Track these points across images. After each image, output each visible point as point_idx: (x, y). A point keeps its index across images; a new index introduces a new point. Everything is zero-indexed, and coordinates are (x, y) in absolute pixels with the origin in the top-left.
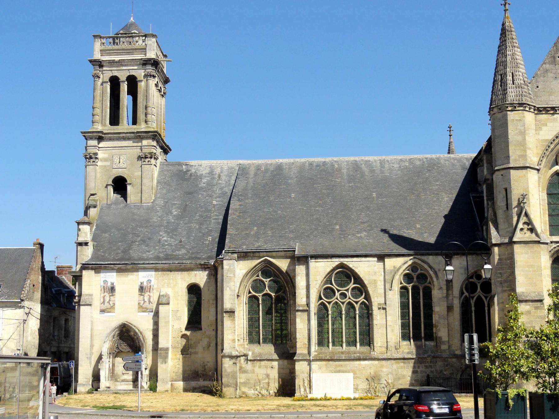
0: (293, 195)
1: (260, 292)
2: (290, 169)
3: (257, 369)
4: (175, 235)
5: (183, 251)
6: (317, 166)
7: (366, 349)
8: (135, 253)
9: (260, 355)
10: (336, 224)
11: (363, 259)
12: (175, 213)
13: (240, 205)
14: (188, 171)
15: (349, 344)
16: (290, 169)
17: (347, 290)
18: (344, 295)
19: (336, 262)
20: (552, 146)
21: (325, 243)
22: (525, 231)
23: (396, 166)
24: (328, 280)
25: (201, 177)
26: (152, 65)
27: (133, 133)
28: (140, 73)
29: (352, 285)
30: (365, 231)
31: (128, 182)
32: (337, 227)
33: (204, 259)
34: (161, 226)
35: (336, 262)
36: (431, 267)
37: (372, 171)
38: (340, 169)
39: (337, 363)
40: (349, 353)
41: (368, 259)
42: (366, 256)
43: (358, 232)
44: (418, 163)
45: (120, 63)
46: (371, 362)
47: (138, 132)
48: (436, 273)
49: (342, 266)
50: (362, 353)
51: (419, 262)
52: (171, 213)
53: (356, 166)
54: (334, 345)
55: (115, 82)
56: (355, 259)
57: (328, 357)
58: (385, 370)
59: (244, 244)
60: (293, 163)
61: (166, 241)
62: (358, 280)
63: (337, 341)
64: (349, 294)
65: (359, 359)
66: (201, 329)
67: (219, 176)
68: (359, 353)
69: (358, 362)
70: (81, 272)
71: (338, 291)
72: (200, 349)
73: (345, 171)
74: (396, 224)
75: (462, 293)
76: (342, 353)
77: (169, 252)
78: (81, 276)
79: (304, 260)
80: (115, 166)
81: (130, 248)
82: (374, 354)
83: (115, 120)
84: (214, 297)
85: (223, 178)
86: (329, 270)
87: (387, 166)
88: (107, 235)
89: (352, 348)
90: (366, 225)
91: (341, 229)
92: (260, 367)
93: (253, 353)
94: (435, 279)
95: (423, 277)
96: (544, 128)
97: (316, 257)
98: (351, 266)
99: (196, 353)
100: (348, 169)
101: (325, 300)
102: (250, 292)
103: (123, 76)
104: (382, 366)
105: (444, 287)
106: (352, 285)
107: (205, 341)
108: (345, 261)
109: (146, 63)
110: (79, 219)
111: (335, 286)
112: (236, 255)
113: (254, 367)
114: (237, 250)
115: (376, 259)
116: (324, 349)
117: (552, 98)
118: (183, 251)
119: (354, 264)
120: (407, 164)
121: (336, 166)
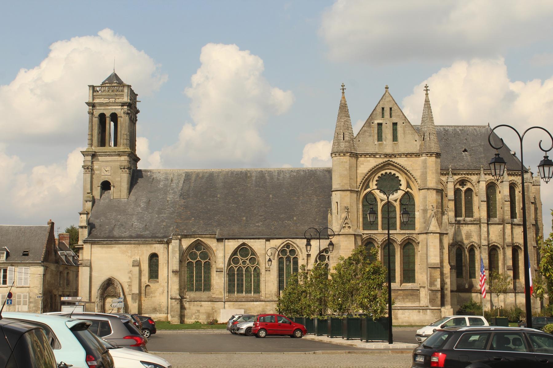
0: (219, 196)
1: (194, 260)
2: (218, 176)
3: (192, 307)
4: (143, 221)
5: (147, 232)
6: (236, 174)
7: (256, 295)
8: (116, 233)
9: (194, 298)
10: (244, 216)
11: (257, 240)
12: (142, 206)
13: (184, 202)
14: (151, 176)
15: (247, 292)
16: (218, 176)
17: (247, 259)
18: (244, 262)
19: (241, 242)
20: (366, 177)
21: (236, 229)
22: (347, 228)
23: (288, 175)
24: (235, 253)
25: (159, 181)
26: (128, 106)
27: (115, 152)
28: (120, 111)
29: (249, 257)
30: (261, 221)
31: (112, 184)
32: (244, 218)
33: (160, 238)
34: (133, 215)
35: (241, 242)
36: (298, 246)
37: (272, 178)
38: (251, 176)
39: (240, 303)
40: (247, 297)
41: (260, 240)
42: (259, 239)
43: (257, 222)
44: (302, 173)
45: (107, 104)
46: (260, 303)
47: (118, 152)
48: (301, 250)
49: (244, 244)
50: (255, 298)
51: (291, 243)
52: (140, 206)
53: (262, 175)
54: (238, 292)
55: (102, 117)
56: (252, 240)
57: (234, 300)
58: (268, 308)
59: (185, 229)
60: (221, 172)
61: (136, 225)
62: (254, 253)
63: (240, 291)
64: (248, 262)
65: (254, 301)
66: (158, 282)
67: (172, 180)
68: (253, 297)
69: (252, 303)
70: (83, 245)
71: (242, 259)
72: (157, 294)
73: (254, 178)
74: (282, 216)
75: (316, 261)
76: (243, 297)
77: (139, 233)
78: (82, 248)
79: (219, 240)
80: (103, 174)
81: (113, 229)
82: (262, 298)
83: (102, 142)
84: (167, 261)
85: (175, 181)
86: (236, 247)
87: (282, 175)
88: (98, 221)
89: (249, 295)
90: (263, 217)
91: (247, 220)
92: (194, 305)
93: (190, 297)
94: (300, 253)
95: (293, 252)
96: (362, 166)
97: (228, 239)
98: (249, 245)
99: (155, 297)
100: (256, 177)
101: (233, 265)
102: (188, 260)
103: (108, 114)
104: (267, 306)
105: (306, 258)
106: (249, 257)
107: (160, 290)
108: (246, 241)
109: (123, 104)
110: (80, 212)
111: (239, 256)
112: (179, 237)
113: (190, 305)
114: (181, 234)
115: (265, 240)
116: (232, 295)
117: (367, 148)
118: (147, 232)
119: (250, 243)
120: (295, 174)
121: (249, 175)
